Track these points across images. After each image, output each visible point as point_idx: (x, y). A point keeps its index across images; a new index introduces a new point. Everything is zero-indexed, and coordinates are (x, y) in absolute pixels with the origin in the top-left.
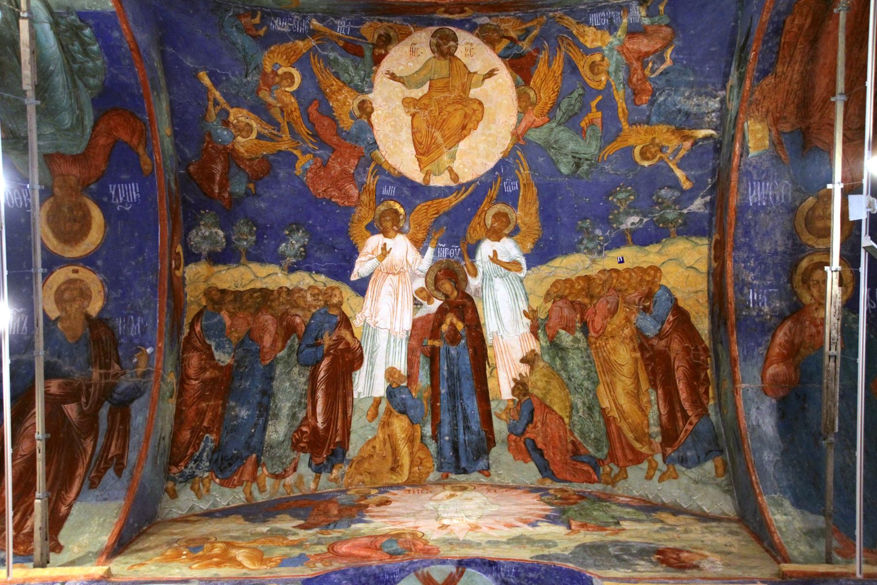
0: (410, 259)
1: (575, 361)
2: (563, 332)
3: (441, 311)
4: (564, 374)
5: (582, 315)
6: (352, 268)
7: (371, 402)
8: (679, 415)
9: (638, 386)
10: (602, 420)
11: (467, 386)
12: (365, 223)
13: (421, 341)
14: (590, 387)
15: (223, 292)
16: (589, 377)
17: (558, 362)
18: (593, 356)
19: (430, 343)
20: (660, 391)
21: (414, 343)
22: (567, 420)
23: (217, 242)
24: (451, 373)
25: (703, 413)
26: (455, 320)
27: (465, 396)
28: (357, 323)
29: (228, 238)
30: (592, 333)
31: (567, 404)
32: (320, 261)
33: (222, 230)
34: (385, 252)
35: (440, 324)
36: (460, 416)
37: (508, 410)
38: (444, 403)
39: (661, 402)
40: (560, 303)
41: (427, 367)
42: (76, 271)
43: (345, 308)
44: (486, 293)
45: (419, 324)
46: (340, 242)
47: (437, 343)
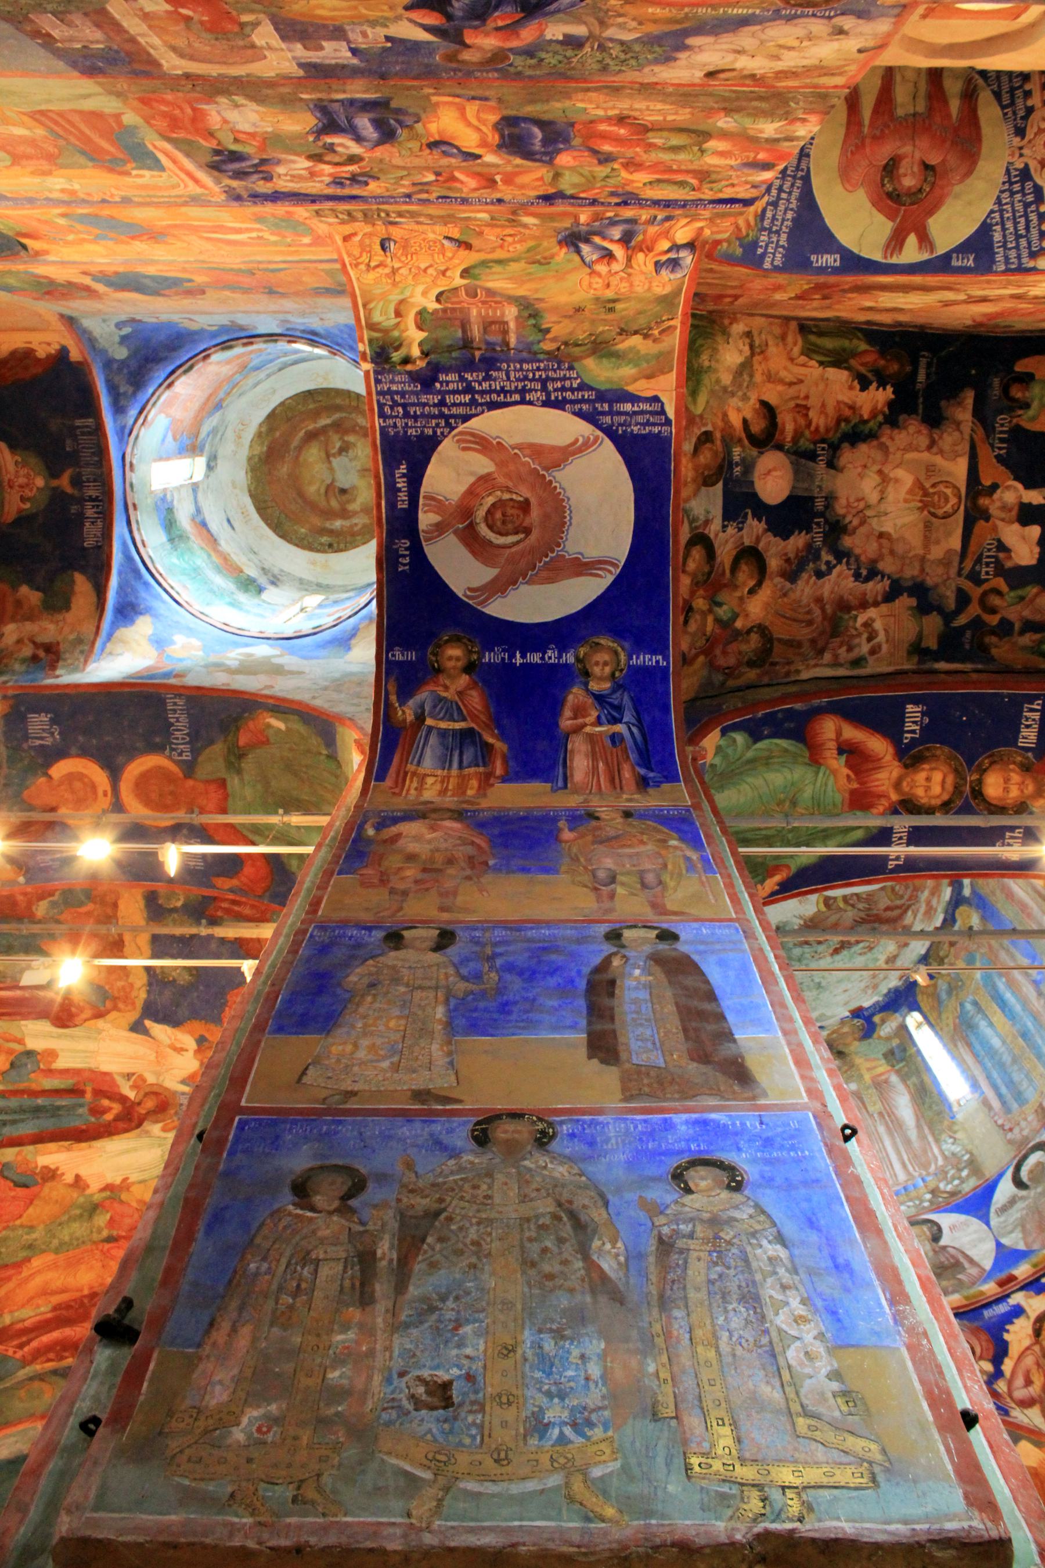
0: (175, 1072)
1: (78, 1229)
2: (108, 1216)
3: (123, 1099)
4: (65, 1218)
5: (124, 1237)
6: (157, 1021)
7: (19, 1036)
8: (24, 1339)
9: (54, 1293)
10: (19, 1259)
11: (48, 1124)
12: (207, 1035)
13: (91, 1080)
14: (53, 1246)
15: (115, 905)
16: (62, 1244)
17: (78, 1212)
18: (83, 1248)
19: (89, 1089)
20: (49, 1315)
21: (86, 1074)
22: (18, 1222)
23: (169, 899)
24: (59, 1108)
25: (25, 1362)
26: (115, 1112)
27: (36, 1121)
28: (100, 1023)
29: (174, 910)
30: (107, 1246)
31: (35, 1223)
32: (161, 994)
33: (183, 906)
34: (180, 1050)
35: (109, 1098)
36: (16, 1117)
37: (27, 1162)
38: (27, 1101)
39: (38, 1318)
40: (136, 1216)
41: (62, 1087)
42: (105, 794)
43: (114, 1014)
44: (145, 1141)
45: (108, 1078)
46: (183, 1011)
47: (89, 1096)
